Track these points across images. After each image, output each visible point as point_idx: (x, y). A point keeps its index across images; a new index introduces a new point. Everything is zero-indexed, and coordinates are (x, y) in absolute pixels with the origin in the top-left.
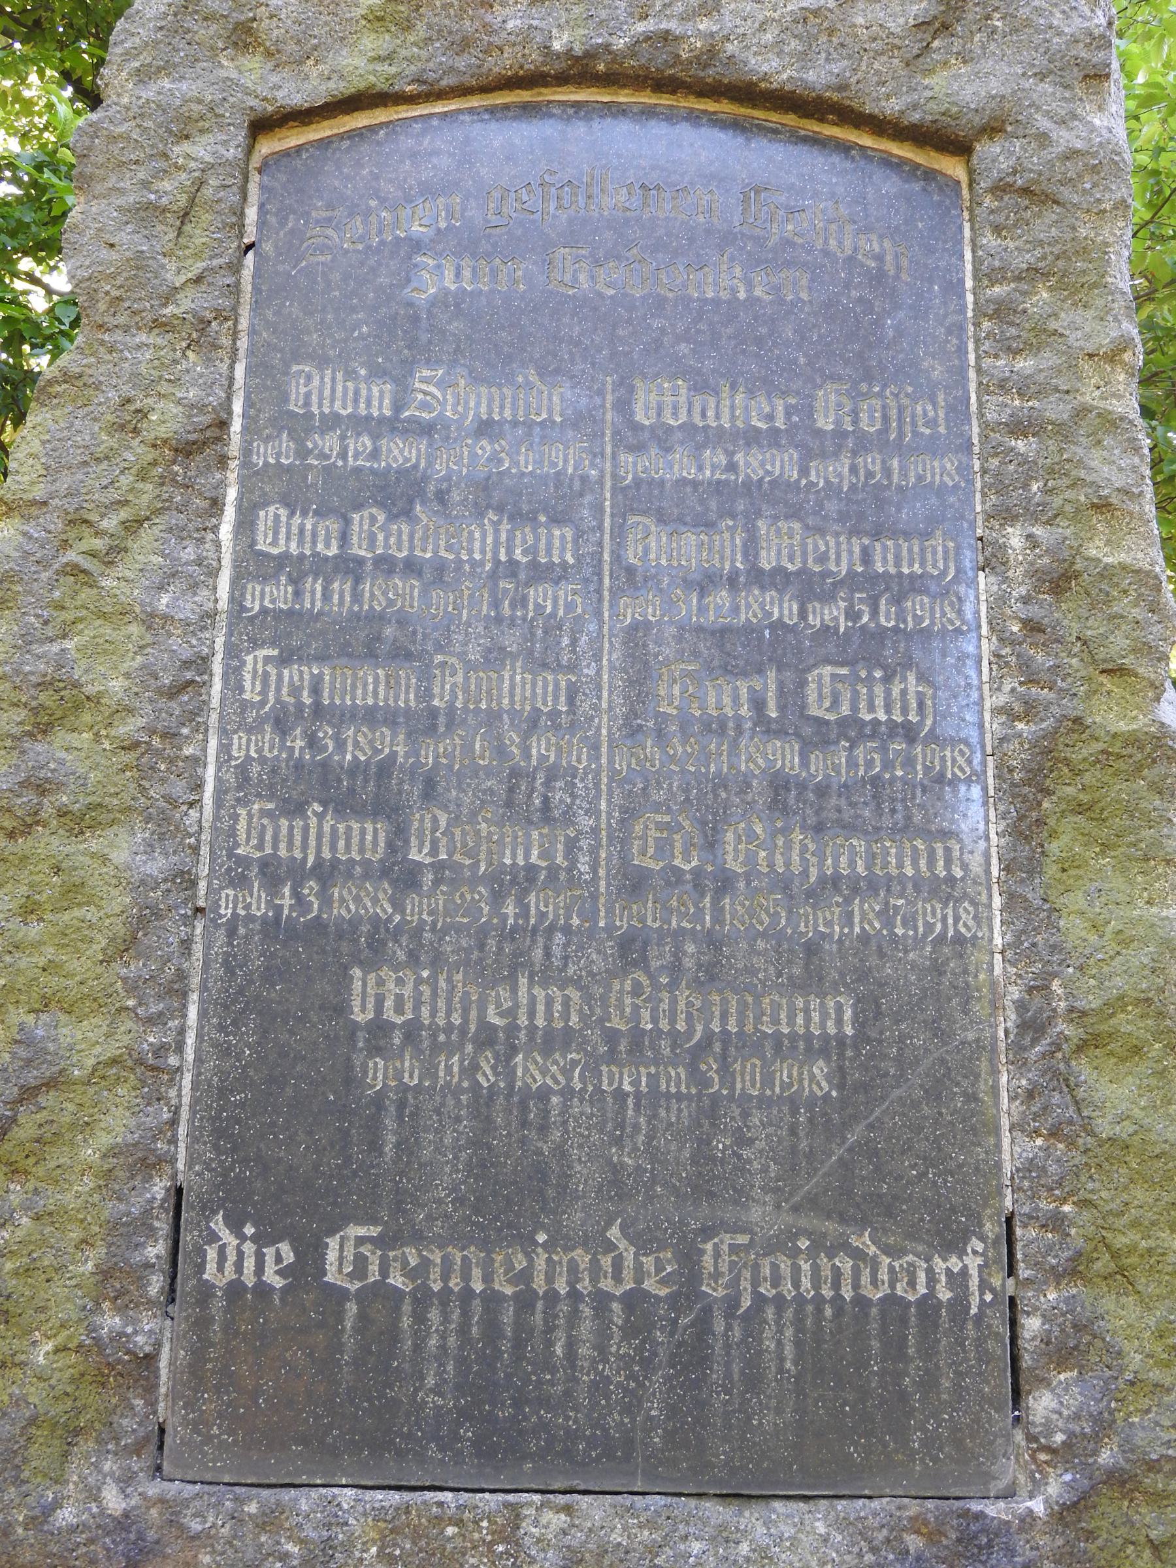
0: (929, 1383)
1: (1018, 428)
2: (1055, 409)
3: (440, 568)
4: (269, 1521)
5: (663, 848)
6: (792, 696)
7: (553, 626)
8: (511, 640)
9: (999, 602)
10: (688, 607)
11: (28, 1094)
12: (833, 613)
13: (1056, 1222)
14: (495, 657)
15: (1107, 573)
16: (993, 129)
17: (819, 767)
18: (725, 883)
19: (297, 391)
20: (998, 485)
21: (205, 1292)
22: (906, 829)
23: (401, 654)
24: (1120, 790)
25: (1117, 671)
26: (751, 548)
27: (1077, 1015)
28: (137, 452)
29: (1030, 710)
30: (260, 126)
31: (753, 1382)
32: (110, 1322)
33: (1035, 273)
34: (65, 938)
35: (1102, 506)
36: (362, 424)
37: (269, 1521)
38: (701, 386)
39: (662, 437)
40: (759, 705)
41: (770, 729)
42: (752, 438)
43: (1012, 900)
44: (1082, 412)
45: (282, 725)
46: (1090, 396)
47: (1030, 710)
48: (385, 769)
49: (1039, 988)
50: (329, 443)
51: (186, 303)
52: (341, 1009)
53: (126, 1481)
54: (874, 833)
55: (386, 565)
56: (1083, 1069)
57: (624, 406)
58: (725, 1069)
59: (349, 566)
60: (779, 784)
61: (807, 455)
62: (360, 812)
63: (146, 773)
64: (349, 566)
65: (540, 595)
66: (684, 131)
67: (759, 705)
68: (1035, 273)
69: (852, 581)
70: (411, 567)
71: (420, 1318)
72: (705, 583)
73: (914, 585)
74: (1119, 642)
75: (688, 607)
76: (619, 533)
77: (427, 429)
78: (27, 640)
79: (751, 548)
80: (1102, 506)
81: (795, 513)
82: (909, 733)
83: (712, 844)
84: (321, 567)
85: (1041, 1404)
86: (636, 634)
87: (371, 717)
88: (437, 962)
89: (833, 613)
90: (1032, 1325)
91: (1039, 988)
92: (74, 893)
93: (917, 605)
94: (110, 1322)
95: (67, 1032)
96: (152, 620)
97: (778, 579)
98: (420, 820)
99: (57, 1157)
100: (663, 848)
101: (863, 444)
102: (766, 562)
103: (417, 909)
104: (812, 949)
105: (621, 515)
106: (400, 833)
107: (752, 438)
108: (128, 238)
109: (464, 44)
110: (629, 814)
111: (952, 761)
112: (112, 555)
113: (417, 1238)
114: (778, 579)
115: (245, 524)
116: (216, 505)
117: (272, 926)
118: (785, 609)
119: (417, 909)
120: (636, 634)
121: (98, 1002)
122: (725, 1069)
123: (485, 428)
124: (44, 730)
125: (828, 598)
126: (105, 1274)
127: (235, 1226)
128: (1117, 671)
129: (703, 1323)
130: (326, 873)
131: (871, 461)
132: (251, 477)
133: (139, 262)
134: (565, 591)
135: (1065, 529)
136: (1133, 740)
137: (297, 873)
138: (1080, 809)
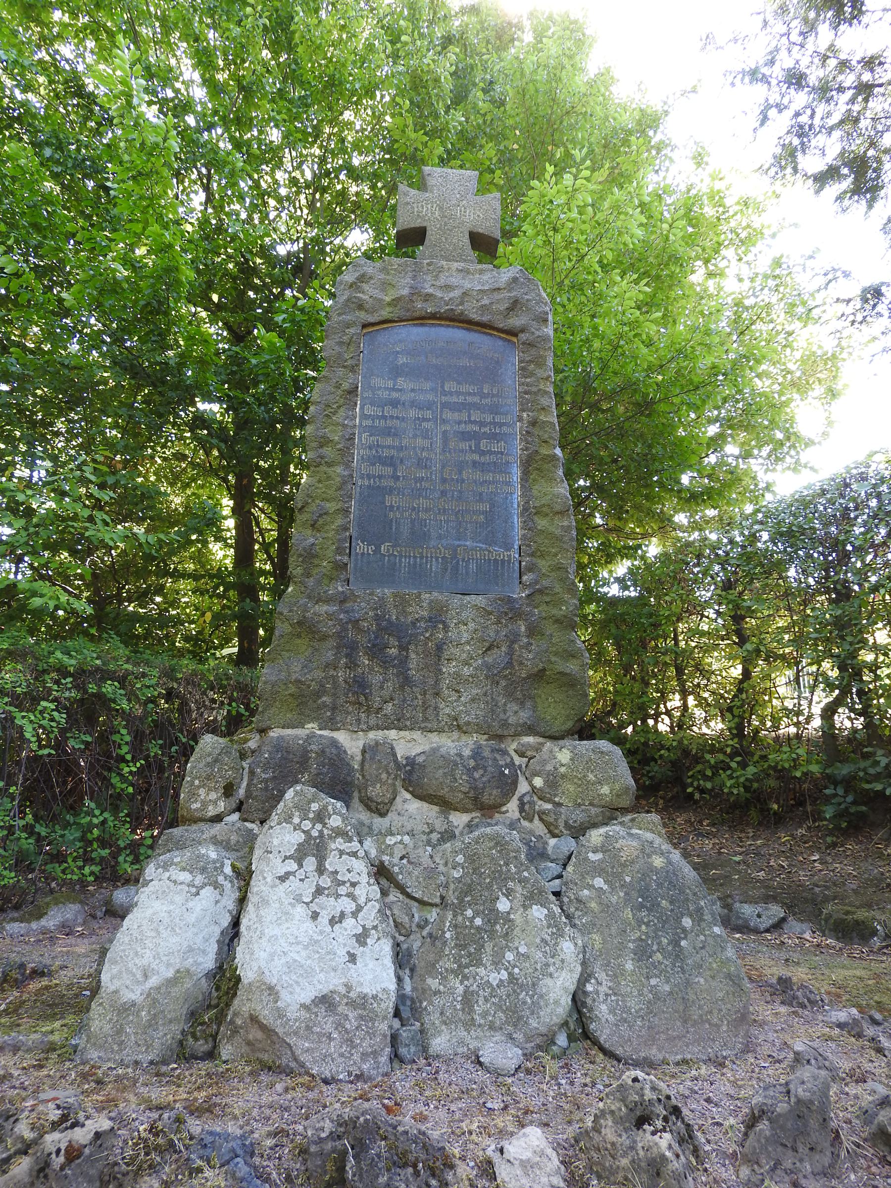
0: (503, 574)
1: (526, 393)
2: (534, 389)
3: (403, 418)
4: (371, 594)
5: (450, 474)
6: (477, 445)
7: (427, 430)
8: (418, 433)
9: (521, 428)
10: (456, 427)
11: (321, 515)
12: (487, 429)
13: (529, 546)
14: (415, 436)
15: (544, 422)
16: (522, 331)
17: (483, 459)
18: (463, 481)
19: (373, 382)
20: (522, 404)
21: (357, 554)
22: (501, 472)
23: (395, 435)
24: (546, 466)
25: (545, 442)
26: (469, 416)
27: (535, 507)
28: (340, 392)
29: (527, 449)
30: (364, 326)
31: (467, 573)
32: (339, 558)
33: (530, 362)
34: (327, 487)
35: (543, 409)
36: (386, 389)
37: (371, 594)
38: (459, 383)
39: (451, 393)
40: (470, 447)
41: (473, 452)
42: (470, 394)
43: (522, 486)
44: (539, 390)
45: (370, 448)
46: (542, 387)
47: (527, 449)
48: (392, 457)
49: (527, 502)
50: (380, 393)
51: (349, 363)
52: (384, 503)
53: (342, 586)
54: (494, 472)
55: (392, 417)
56: (536, 518)
57: (443, 387)
58: (463, 516)
59: (384, 417)
60: (474, 463)
61: (482, 397)
62: (387, 465)
63: (343, 456)
64: (384, 417)
65: (424, 424)
66: (456, 330)
67: (470, 447)
68: (530, 362)
69: (490, 423)
70: (397, 418)
71: (400, 561)
72: (460, 423)
73: (504, 424)
74: (546, 436)
75: (456, 427)
76: (441, 412)
77: (401, 390)
78: (318, 429)
79: (469, 416)
80: (543, 409)
81: (479, 409)
82: (502, 453)
83: (460, 473)
84: (378, 417)
85: (525, 578)
86: (445, 433)
87: (389, 447)
88: (403, 495)
89: (487, 429)
90: (523, 563)
91: (527, 502)
92: (329, 478)
93: (504, 428)
94: (339, 558)
95: (328, 505)
96: (344, 426)
97: (475, 422)
98: (400, 467)
99: (327, 527)
100: (450, 474)
101: (493, 396)
102: (473, 419)
103: (399, 484)
104: (481, 494)
105: (442, 409)
106: (395, 470)
107: (470, 394)
108: (336, 348)
109: (408, 310)
110: (443, 467)
111: (511, 459)
112: (334, 413)
113: (399, 546)
114: (475, 422)
115: (362, 408)
116: (356, 404)
117: (369, 487)
118: (476, 428)
119: (399, 484)
120: (445, 433)
121: (334, 499)
122: (463, 516)
123: (413, 390)
124: (321, 447)
125: (485, 426)
126: (337, 549)
127: (363, 542)
128: (545, 442)
129: (458, 563)
130: (380, 477)
131: (495, 399)
132: (363, 399)
133: (339, 353)
134: (430, 423)
135: (535, 413)
136: (548, 456)
137: (374, 477)
138: (537, 469)
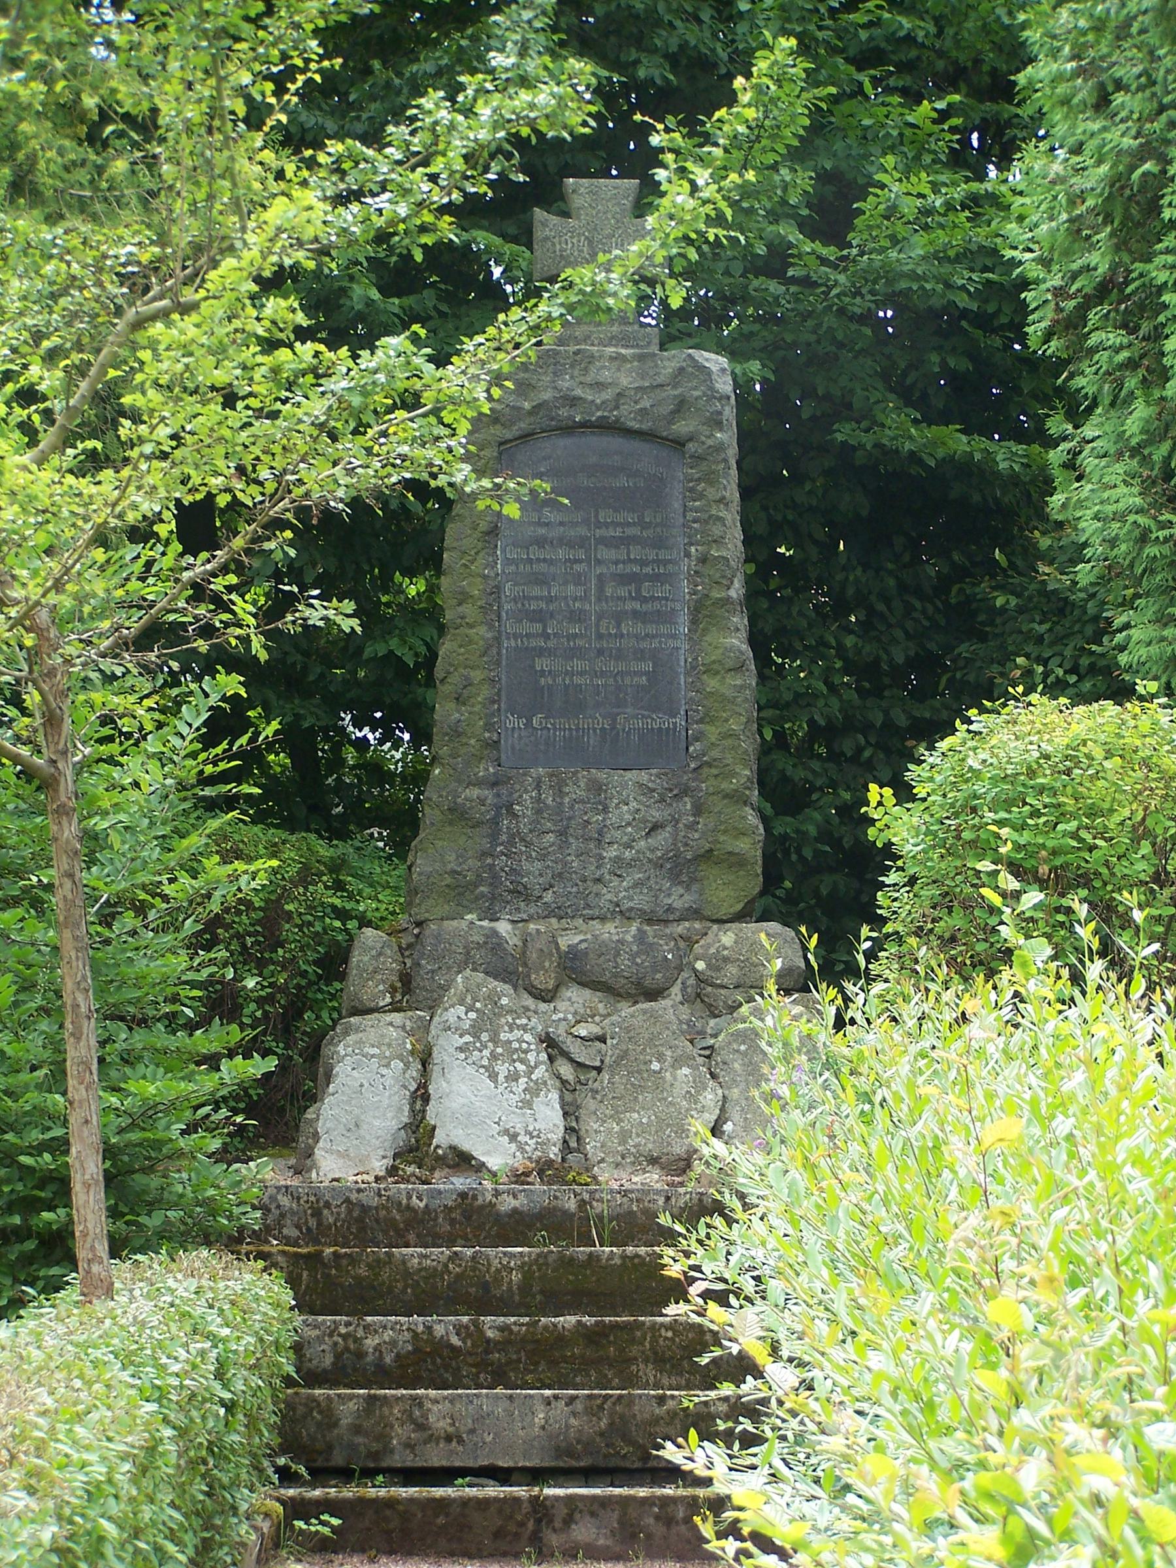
6: (638, 590)
7: (579, 574)
8: (570, 578)
12: (648, 570)
16: (691, 439)
18: (622, 636)
24: (718, 612)
26: (628, 554)
28: (477, 534)
30: (501, 444)
33: (699, 480)
38: (616, 510)
39: (607, 525)
41: (633, 599)
42: (629, 524)
44: (711, 517)
45: (515, 600)
46: (714, 512)
55: (538, 560)
57: (596, 516)
59: (530, 561)
61: (643, 528)
65: (577, 567)
66: (610, 439)
68: (699, 480)
69: (654, 561)
70: (545, 560)
72: (616, 563)
73: (670, 561)
77: (547, 524)
79: (628, 554)
82: (667, 599)
83: (618, 626)
86: (600, 577)
87: (537, 598)
89: (648, 570)
92: (471, 642)
93: (670, 567)
94: (487, 735)
96: (485, 577)
101: (657, 525)
107: (629, 524)
109: (552, 419)
114: (635, 561)
115: (503, 551)
118: (636, 569)
119: (550, 644)
120: (600, 577)
123: (561, 524)
124: (460, 604)
125: (647, 565)
131: (659, 530)
